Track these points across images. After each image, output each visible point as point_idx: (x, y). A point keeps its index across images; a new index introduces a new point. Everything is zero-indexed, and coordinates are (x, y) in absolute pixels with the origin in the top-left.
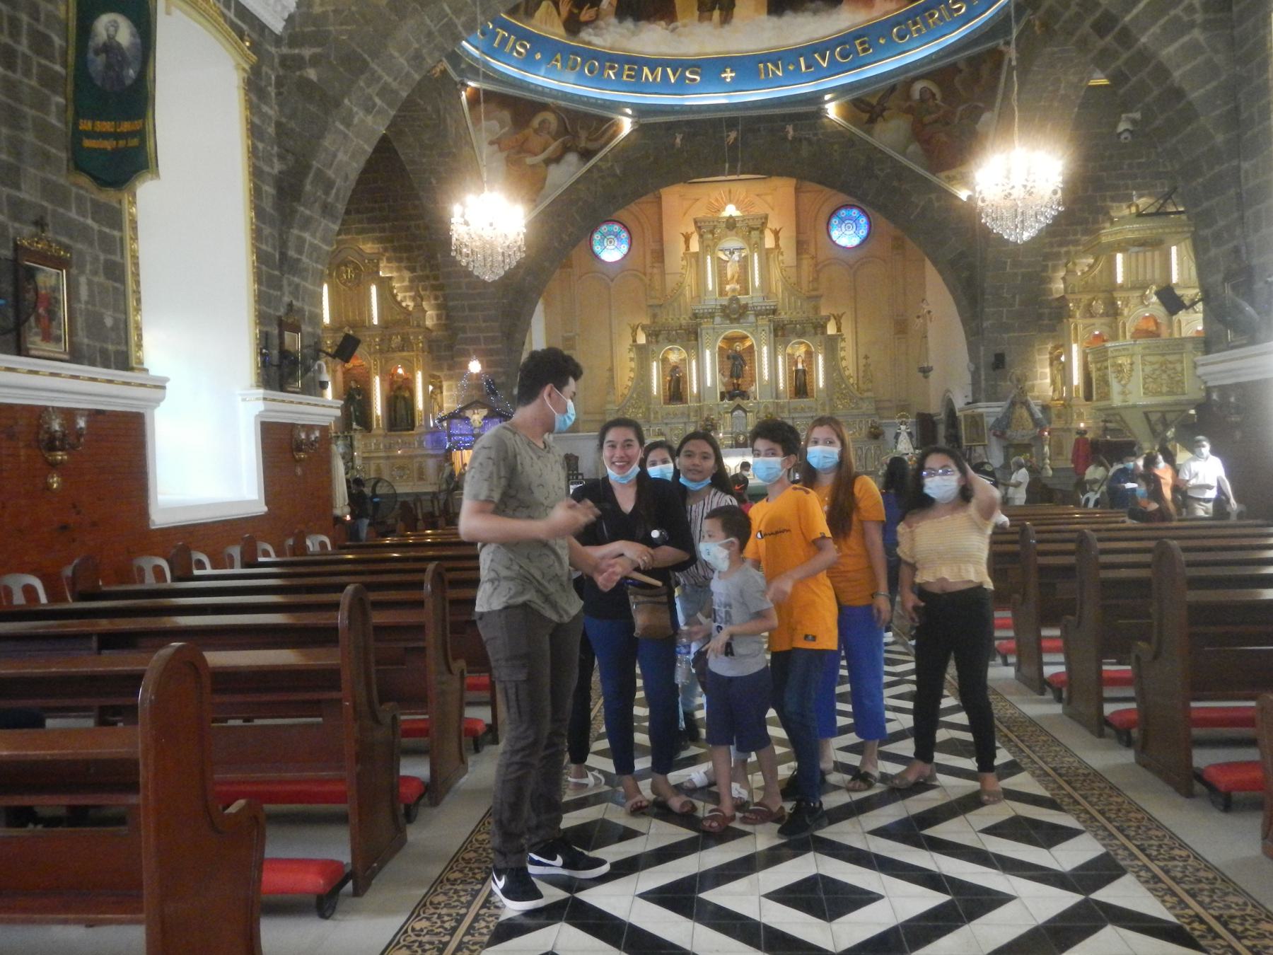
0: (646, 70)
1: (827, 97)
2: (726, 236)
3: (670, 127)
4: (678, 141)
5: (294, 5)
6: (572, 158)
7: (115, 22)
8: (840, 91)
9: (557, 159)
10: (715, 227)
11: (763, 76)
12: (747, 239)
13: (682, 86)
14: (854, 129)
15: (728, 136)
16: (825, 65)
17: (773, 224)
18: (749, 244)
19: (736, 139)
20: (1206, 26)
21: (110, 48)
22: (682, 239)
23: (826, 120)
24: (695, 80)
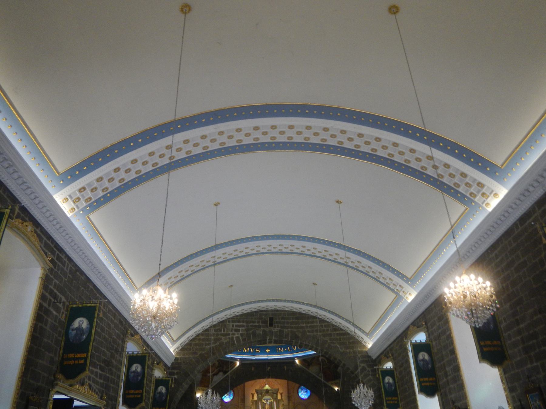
0: (245, 349)
1: (296, 358)
2: (266, 396)
3: (250, 364)
4: (253, 369)
5: (174, 360)
6: (221, 373)
7: (83, 320)
8: (299, 358)
9: (216, 374)
10: (262, 393)
11: (278, 351)
12: (272, 396)
13: (254, 353)
14: (304, 367)
15: (267, 368)
16: (295, 350)
17: (280, 391)
18: (272, 398)
19: (270, 369)
20: (372, 375)
21: (161, 393)
22: (251, 396)
23: (296, 364)
24: (258, 351)
